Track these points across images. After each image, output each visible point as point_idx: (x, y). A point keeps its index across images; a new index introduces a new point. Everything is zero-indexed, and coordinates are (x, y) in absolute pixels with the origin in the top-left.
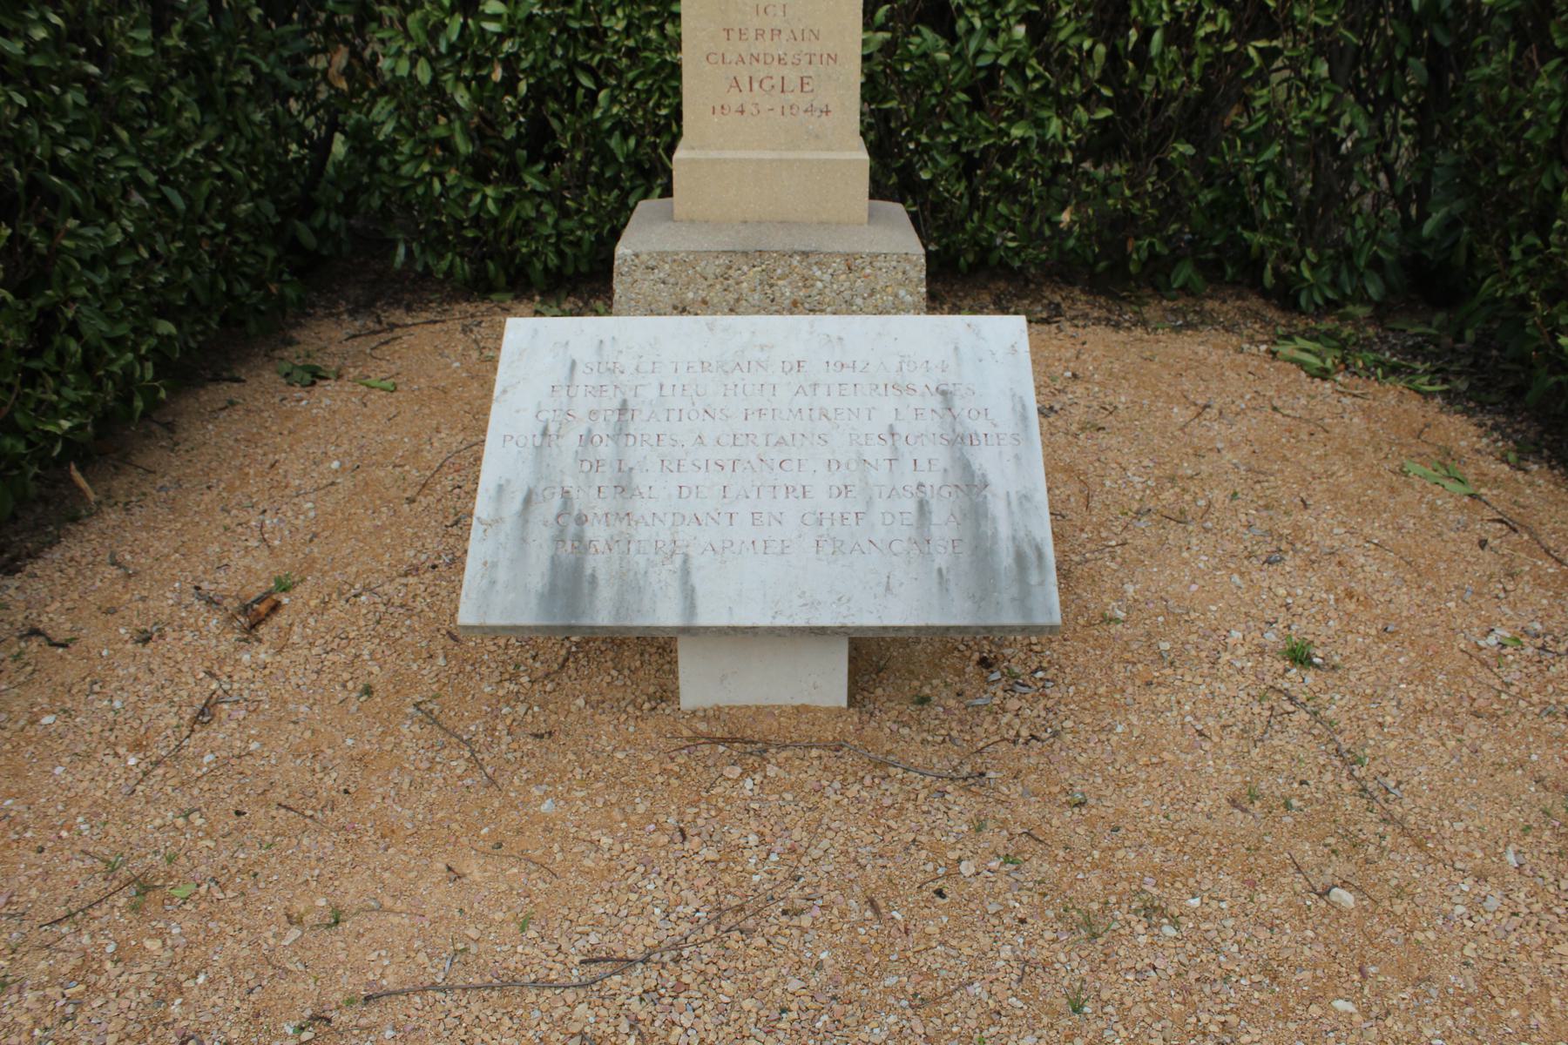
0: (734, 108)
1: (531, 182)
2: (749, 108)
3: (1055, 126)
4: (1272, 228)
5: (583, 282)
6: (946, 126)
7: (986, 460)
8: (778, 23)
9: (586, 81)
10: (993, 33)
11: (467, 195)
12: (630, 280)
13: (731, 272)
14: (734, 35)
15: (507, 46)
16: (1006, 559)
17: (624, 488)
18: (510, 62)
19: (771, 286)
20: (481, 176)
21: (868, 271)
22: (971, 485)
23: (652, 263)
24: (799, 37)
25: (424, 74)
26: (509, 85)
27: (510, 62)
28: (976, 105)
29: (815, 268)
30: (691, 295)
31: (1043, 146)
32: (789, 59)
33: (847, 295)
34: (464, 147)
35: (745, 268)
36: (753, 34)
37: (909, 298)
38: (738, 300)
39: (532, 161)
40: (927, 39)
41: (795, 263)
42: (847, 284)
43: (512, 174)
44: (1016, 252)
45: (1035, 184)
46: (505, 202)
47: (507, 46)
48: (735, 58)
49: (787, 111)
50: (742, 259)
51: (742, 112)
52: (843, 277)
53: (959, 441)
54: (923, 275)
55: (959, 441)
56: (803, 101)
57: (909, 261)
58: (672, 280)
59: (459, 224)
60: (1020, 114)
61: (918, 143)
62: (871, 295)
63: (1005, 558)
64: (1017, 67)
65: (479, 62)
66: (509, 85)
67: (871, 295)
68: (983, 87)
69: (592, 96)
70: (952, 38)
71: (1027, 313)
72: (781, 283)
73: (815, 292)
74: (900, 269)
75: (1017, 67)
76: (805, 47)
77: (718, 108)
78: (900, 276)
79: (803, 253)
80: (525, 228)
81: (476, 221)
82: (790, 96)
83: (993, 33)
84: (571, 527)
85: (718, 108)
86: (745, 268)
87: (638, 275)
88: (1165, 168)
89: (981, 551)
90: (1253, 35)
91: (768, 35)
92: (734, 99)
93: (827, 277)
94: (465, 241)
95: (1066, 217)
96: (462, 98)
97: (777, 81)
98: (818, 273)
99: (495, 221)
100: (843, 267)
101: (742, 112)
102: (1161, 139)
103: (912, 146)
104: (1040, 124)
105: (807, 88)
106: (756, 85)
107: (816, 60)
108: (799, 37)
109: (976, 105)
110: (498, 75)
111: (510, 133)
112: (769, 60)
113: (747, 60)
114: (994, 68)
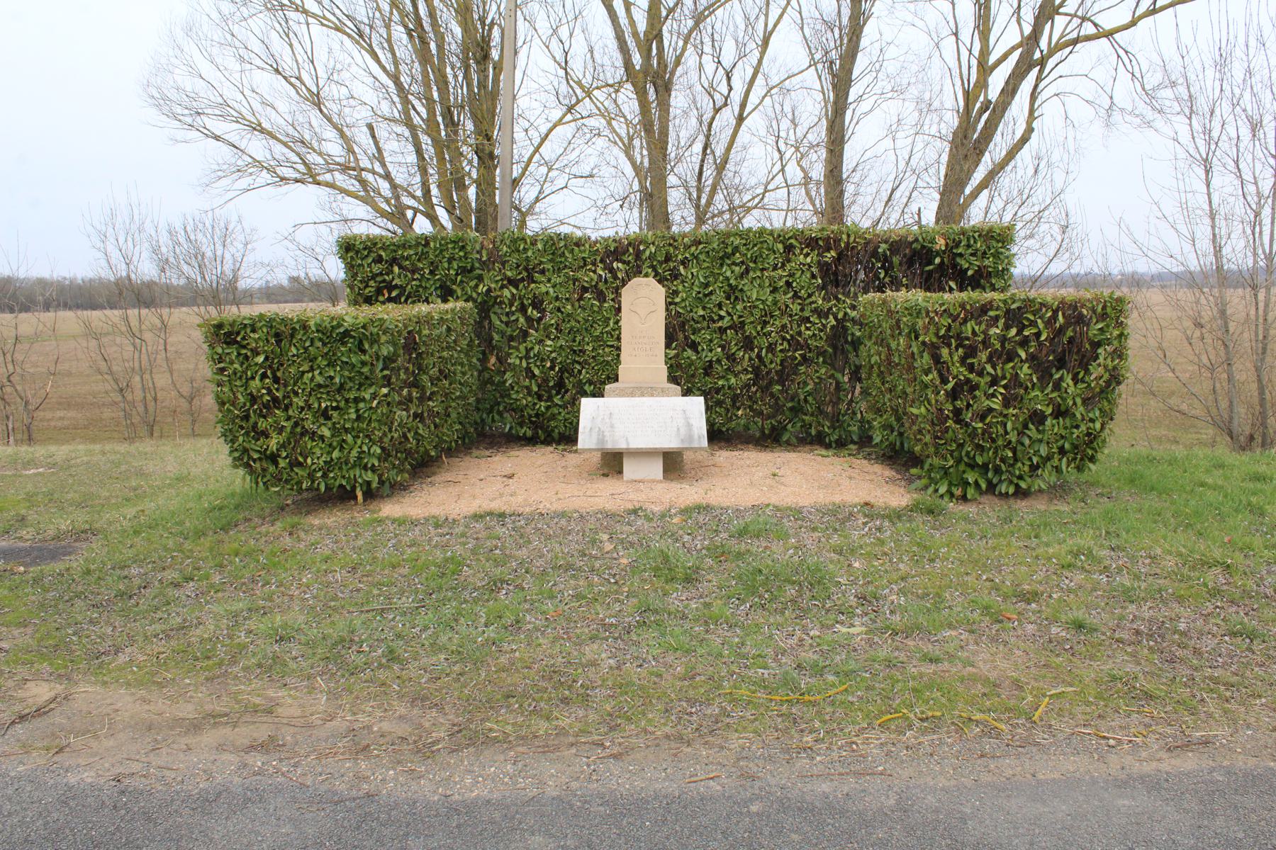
1: (557, 400)
3: (733, 380)
4: (812, 415)
5: (599, 394)
7: (692, 421)
9: (578, 367)
10: (711, 351)
11: (535, 404)
15: (554, 355)
16: (696, 437)
17: (612, 426)
18: (553, 361)
20: (540, 398)
22: (689, 426)
25: (524, 364)
26: (552, 368)
27: (553, 361)
28: (707, 374)
31: (729, 388)
34: (535, 389)
39: (558, 393)
40: (689, 352)
43: (550, 398)
44: (723, 425)
45: (728, 401)
46: (548, 408)
47: (554, 355)
53: (686, 418)
55: (686, 418)
59: (530, 416)
60: (723, 377)
63: (696, 437)
64: (719, 361)
65: (543, 360)
66: (552, 368)
68: (708, 369)
69: (580, 372)
70: (698, 352)
71: (705, 394)
75: (719, 361)
80: (553, 417)
81: (537, 415)
83: (711, 351)
84: (601, 434)
88: (772, 395)
89: (690, 437)
90: (796, 350)
94: (531, 422)
95: (740, 413)
96: (537, 372)
99: (543, 414)
102: (770, 384)
104: (728, 380)
109: (707, 374)
110: (548, 365)
111: (551, 384)
114: (711, 361)
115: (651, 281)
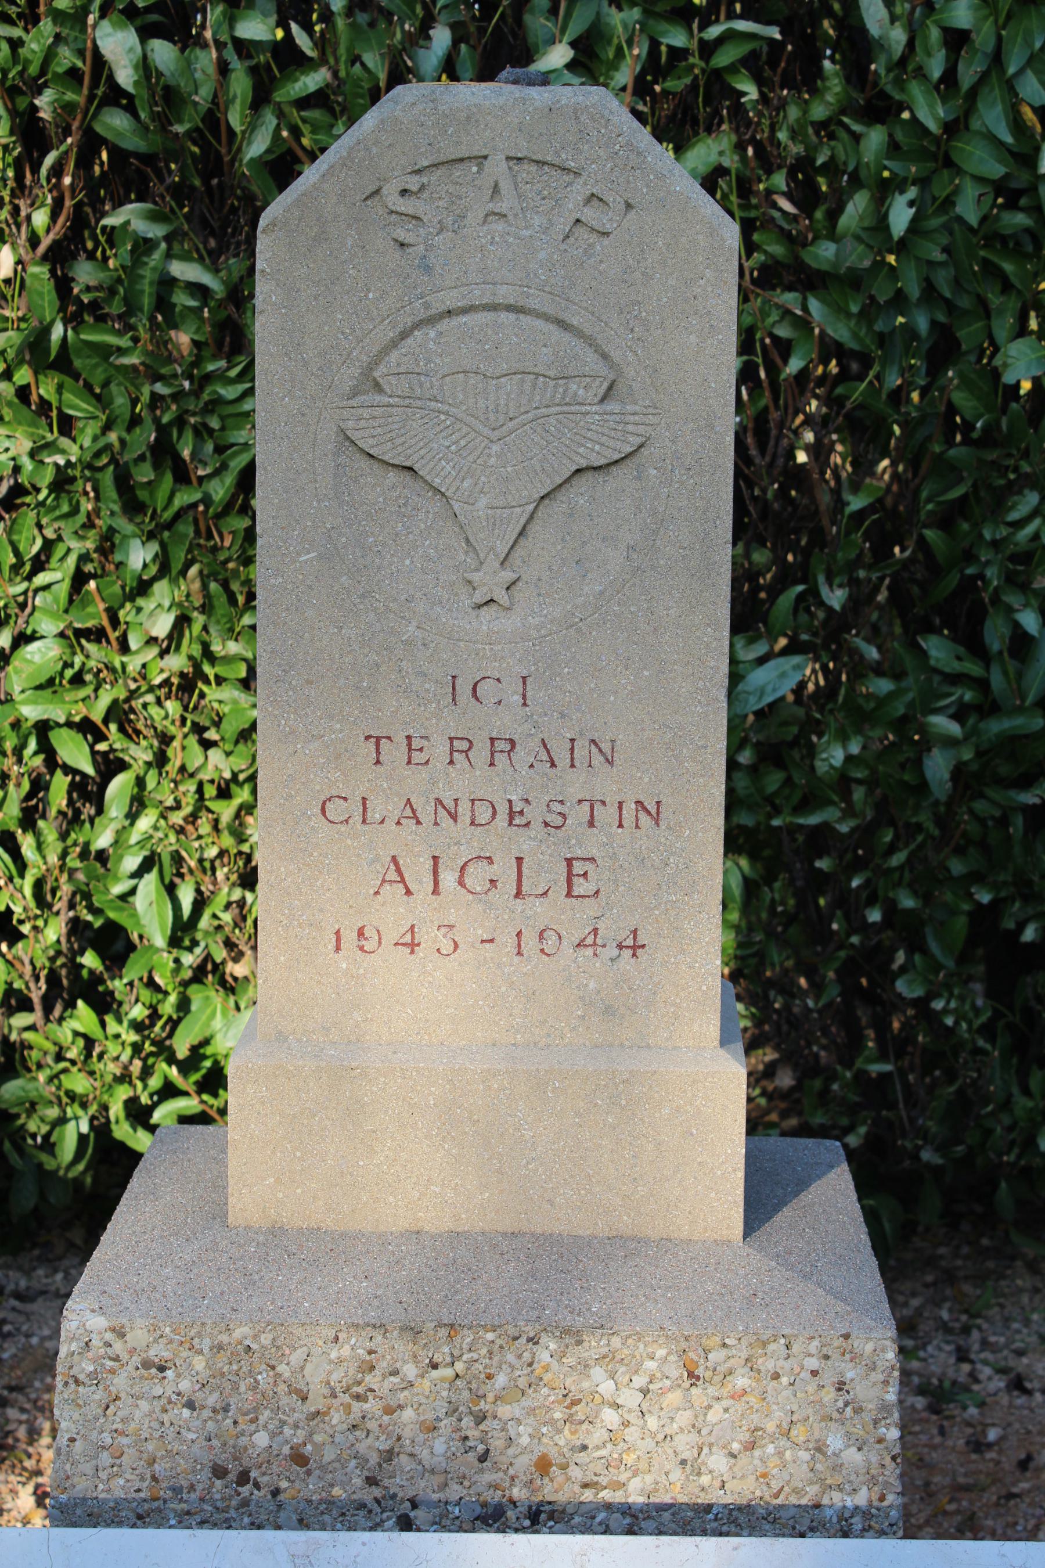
0: (391, 936)
2: (430, 936)
6: (957, 867)
8: (506, 722)
12: (99, 1395)
13: (371, 1380)
14: (394, 752)
19: (480, 1418)
21: (742, 1381)
23: (159, 1352)
24: (562, 757)
29: (598, 1373)
30: (262, 1439)
32: (535, 813)
33: (685, 1444)
35: (410, 1371)
36: (440, 749)
37: (853, 1457)
38: (389, 1455)
41: (544, 1356)
42: (684, 1418)
48: (395, 809)
49: (530, 942)
50: (403, 1347)
51: (413, 946)
52: (674, 1398)
54: (892, 1397)
56: (572, 919)
57: (855, 1357)
58: (212, 1399)
61: (891, 910)
62: (751, 1446)
67: (751, 1446)
72: (505, 1411)
73: (599, 1435)
74: (829, 1378)
76: (575, 785)
77: (349, 937)
78: (829, 1395)
79: (567, 1331)
82: (539, 906)
85: (349, 937)
86: (410, 1371)
87: (120, 1382)
91: (481, 753)
92: (392, 914)
93: (630, 1399)
97: (504, 870)
98: (607, 1387)
100: (675, 1370)
101: (413, 946)
103: (875, 916)
105: (581, 887)
106: (448, 879)
107: (606, 815)
108: (562, 757)
112: (483, 814)
113: (426, 814)
115: (604, 111)
